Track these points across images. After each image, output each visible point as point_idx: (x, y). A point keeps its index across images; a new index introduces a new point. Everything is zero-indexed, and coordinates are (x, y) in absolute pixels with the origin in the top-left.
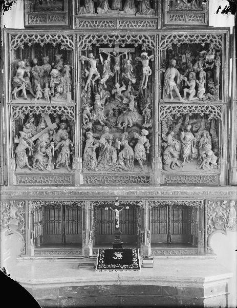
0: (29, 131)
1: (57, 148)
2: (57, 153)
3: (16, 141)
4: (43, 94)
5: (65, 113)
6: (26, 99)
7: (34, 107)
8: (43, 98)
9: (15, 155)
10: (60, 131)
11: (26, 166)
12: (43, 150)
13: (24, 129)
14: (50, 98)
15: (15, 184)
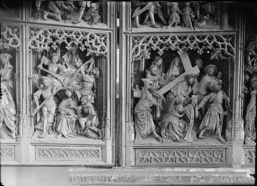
0: (156, 78)
1: (202, 105)
2: (203, 112)
3: (136, 94)
4: (181, 16)
5: (218, 47)
6: (153, 26)
7: (167, 38)
8: (182, 23)
9: (135, 117)
10: (207, 79)
11: (151, 135)
12: (181, 108)
13: (149, 75)
14: (193, 22)
15: (133, 164)
